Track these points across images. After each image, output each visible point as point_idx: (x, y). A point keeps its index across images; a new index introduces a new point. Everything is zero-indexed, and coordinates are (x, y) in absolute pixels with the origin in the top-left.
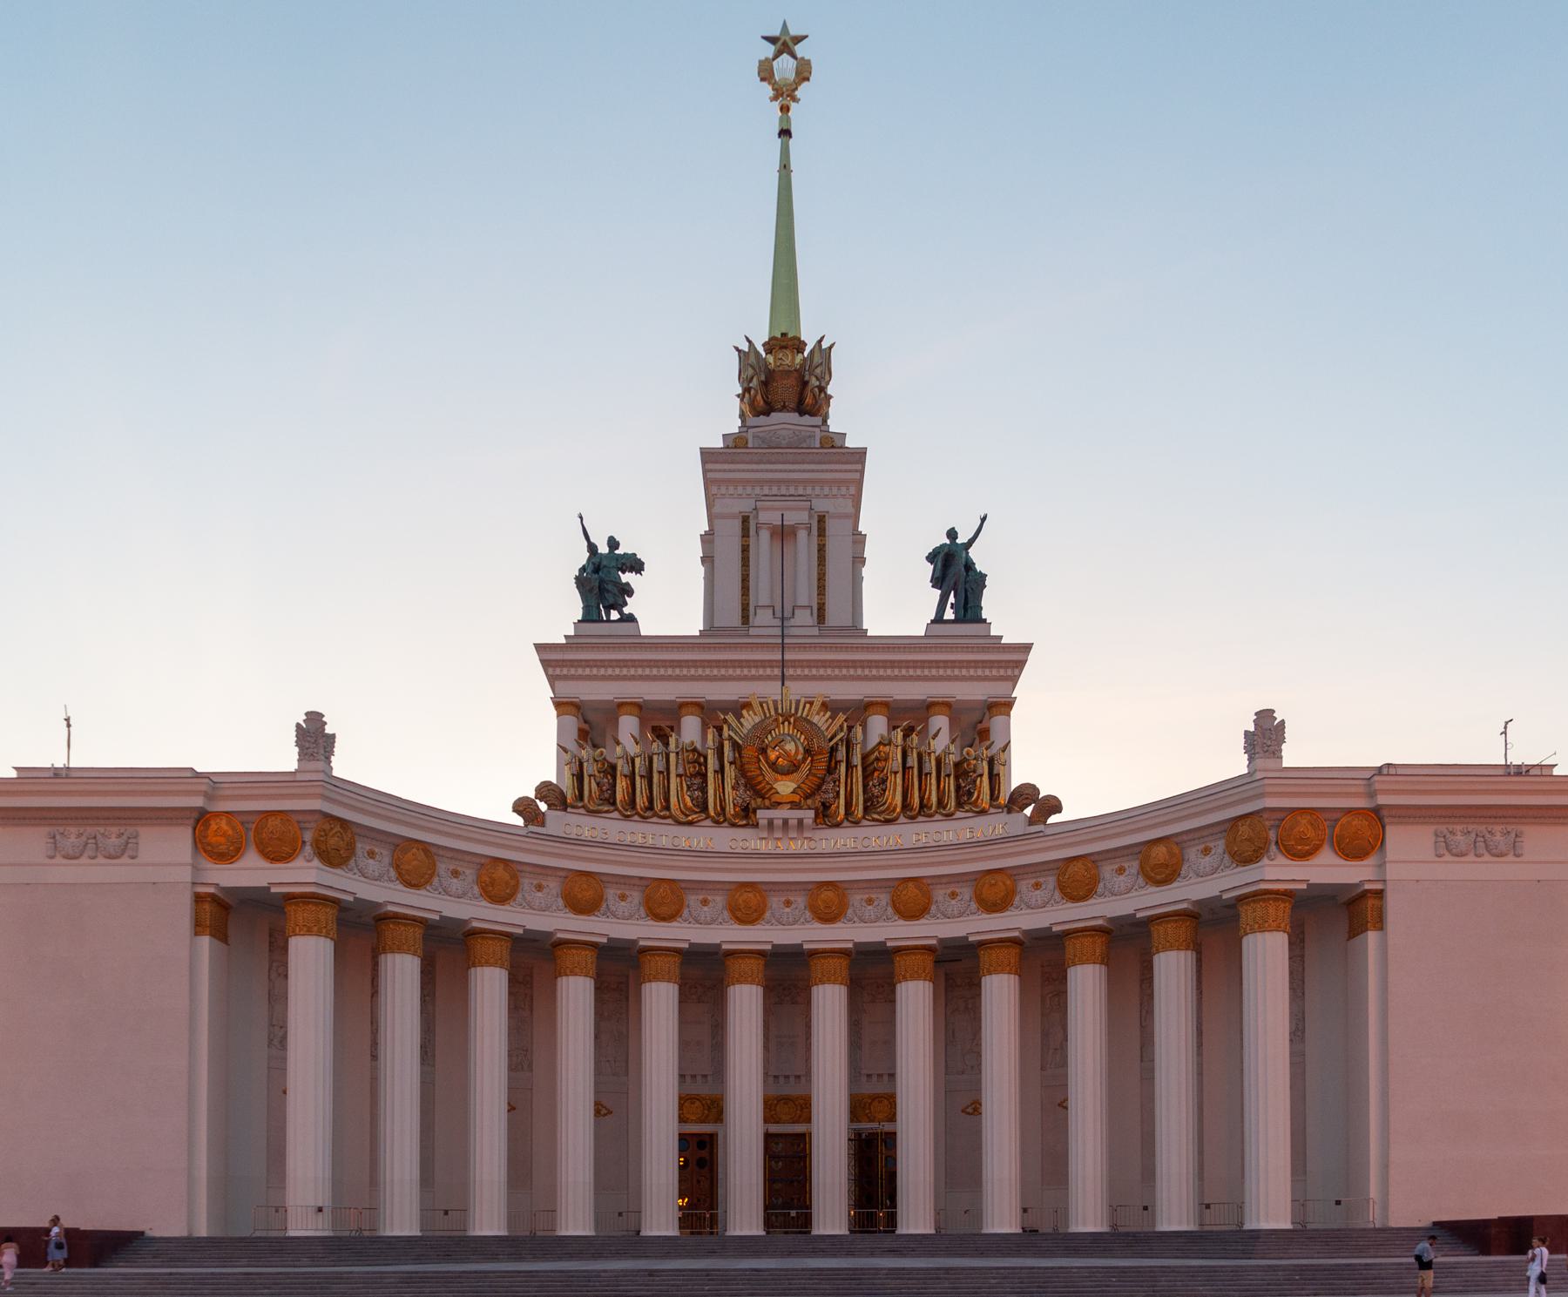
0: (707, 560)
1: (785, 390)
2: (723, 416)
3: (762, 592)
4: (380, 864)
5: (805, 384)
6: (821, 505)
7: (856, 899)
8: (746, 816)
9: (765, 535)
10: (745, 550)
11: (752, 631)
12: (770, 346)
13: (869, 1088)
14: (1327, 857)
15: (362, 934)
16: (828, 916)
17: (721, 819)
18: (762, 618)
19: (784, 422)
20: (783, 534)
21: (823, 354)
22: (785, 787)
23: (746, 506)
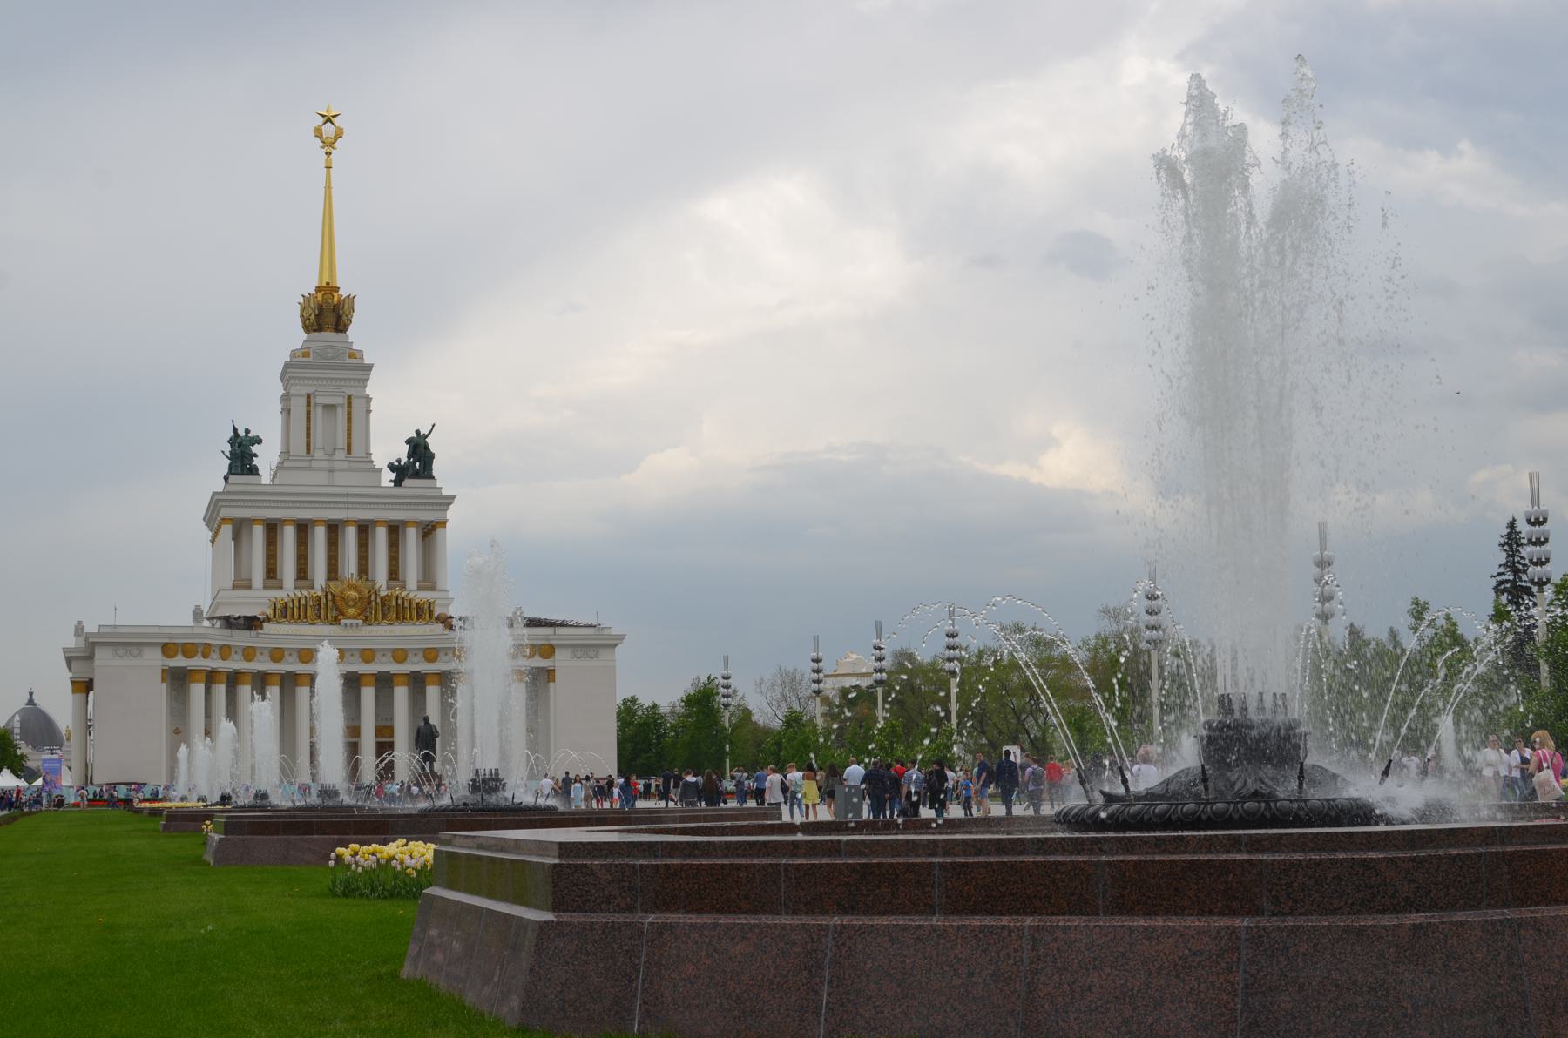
0: (286, 411)
1: (331, 319)
2: (297, 337)
3: (318, 439)
4: (215, 655)
5: (339, 318)
6: (349, 391)
7: (378, 655)
8: (336, 620)
9: (320, 410)
10: (308, 413)
11: (314, 464)
12: (318, 289)
13: (384, 723)
14: (537, 657)
15: (211, 677)
16: (367, 661)
17: (326, 621)
18: (318, 454)
19: (329, 336)
20: (330, 408)
21: (350, 299)
22: (352, 611)
23: (310, 390)
